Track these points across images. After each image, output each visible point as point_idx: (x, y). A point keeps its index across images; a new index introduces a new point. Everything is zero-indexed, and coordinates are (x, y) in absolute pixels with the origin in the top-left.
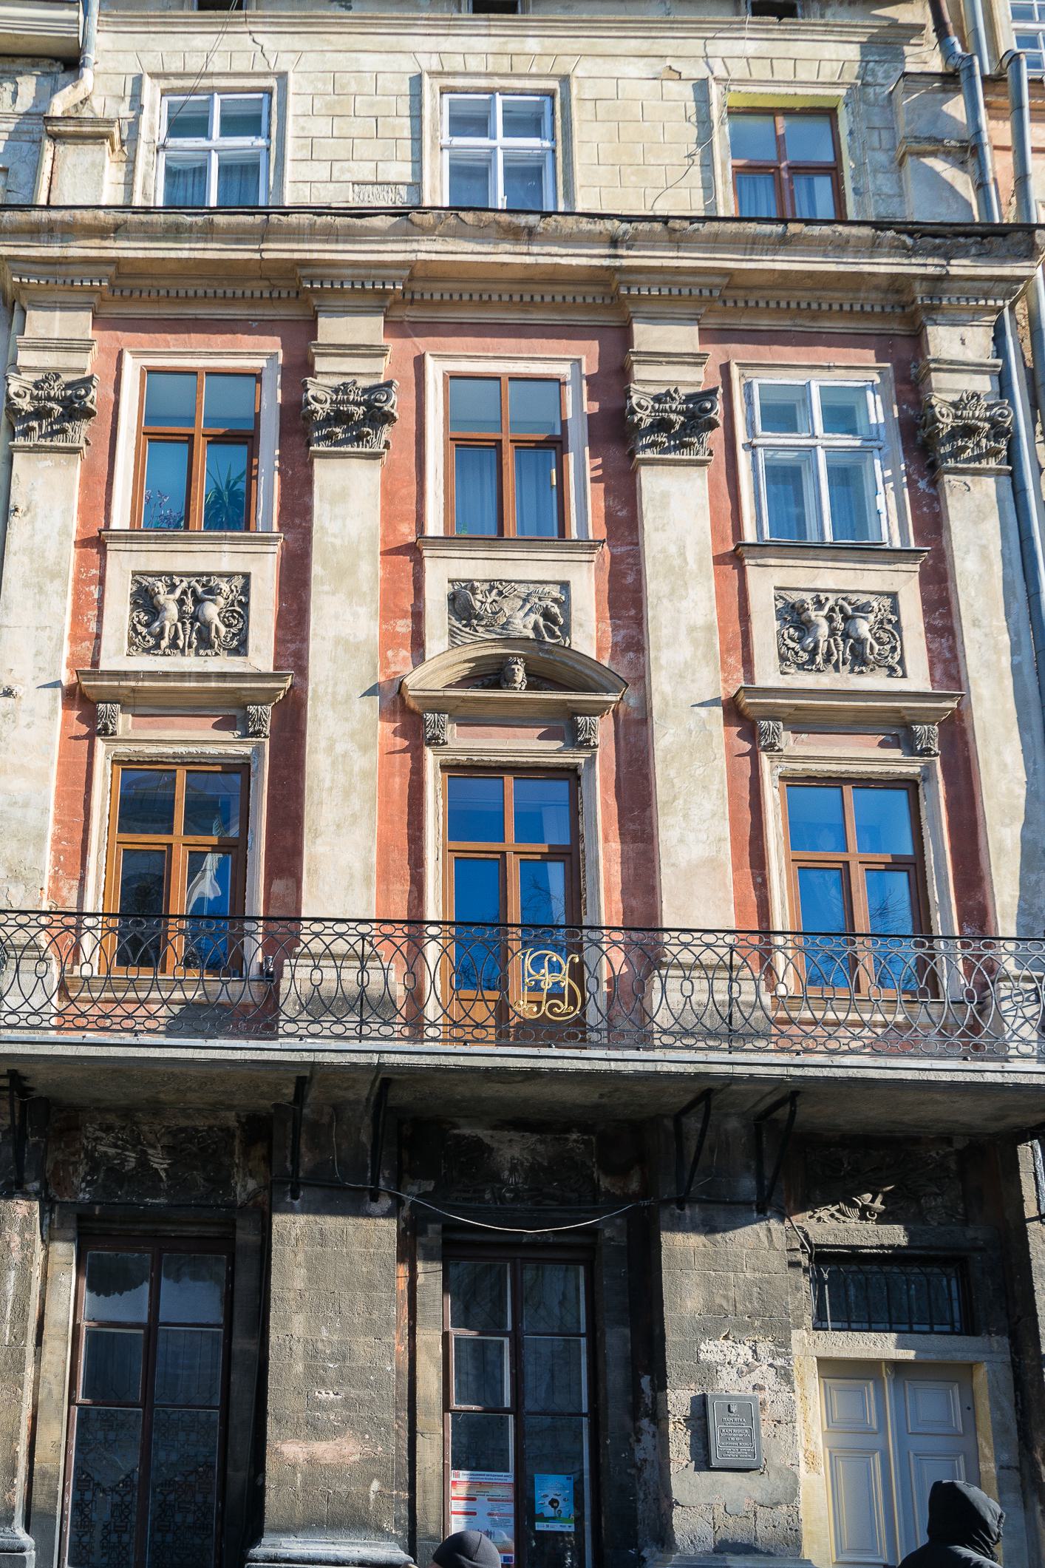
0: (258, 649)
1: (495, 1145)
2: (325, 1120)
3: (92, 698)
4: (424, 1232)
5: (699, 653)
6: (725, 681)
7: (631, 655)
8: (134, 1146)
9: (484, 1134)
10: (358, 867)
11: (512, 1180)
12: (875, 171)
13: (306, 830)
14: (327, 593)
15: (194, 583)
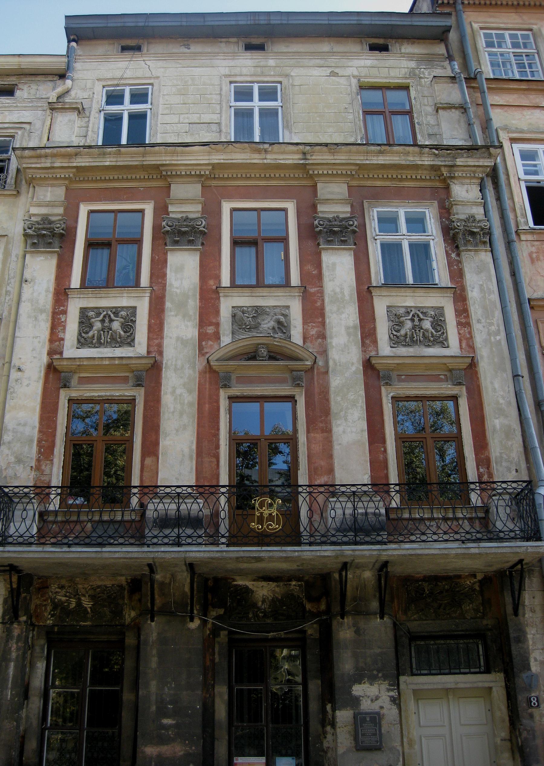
0: (139, 344)
1: (255, 589)
2: (167, 581)
3: (59, 369)
4: (219, 635)
5: (351, 339)
6: (364, 351)
7: (320, 340)
8: (75, 596)
9: (249, 584)
10: (186, 451)
11: (263, 607)
12: (426, 115)
13: (161, 433)
14: (173, 316)
15: (109, 312)
